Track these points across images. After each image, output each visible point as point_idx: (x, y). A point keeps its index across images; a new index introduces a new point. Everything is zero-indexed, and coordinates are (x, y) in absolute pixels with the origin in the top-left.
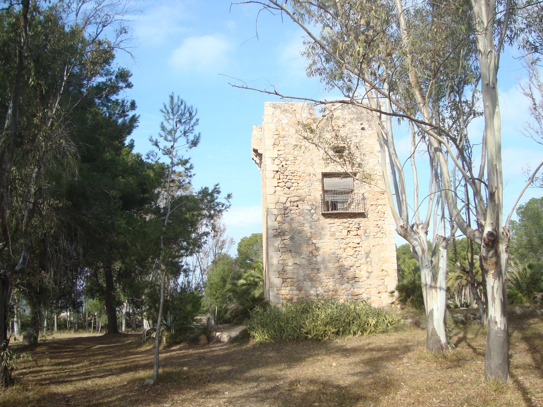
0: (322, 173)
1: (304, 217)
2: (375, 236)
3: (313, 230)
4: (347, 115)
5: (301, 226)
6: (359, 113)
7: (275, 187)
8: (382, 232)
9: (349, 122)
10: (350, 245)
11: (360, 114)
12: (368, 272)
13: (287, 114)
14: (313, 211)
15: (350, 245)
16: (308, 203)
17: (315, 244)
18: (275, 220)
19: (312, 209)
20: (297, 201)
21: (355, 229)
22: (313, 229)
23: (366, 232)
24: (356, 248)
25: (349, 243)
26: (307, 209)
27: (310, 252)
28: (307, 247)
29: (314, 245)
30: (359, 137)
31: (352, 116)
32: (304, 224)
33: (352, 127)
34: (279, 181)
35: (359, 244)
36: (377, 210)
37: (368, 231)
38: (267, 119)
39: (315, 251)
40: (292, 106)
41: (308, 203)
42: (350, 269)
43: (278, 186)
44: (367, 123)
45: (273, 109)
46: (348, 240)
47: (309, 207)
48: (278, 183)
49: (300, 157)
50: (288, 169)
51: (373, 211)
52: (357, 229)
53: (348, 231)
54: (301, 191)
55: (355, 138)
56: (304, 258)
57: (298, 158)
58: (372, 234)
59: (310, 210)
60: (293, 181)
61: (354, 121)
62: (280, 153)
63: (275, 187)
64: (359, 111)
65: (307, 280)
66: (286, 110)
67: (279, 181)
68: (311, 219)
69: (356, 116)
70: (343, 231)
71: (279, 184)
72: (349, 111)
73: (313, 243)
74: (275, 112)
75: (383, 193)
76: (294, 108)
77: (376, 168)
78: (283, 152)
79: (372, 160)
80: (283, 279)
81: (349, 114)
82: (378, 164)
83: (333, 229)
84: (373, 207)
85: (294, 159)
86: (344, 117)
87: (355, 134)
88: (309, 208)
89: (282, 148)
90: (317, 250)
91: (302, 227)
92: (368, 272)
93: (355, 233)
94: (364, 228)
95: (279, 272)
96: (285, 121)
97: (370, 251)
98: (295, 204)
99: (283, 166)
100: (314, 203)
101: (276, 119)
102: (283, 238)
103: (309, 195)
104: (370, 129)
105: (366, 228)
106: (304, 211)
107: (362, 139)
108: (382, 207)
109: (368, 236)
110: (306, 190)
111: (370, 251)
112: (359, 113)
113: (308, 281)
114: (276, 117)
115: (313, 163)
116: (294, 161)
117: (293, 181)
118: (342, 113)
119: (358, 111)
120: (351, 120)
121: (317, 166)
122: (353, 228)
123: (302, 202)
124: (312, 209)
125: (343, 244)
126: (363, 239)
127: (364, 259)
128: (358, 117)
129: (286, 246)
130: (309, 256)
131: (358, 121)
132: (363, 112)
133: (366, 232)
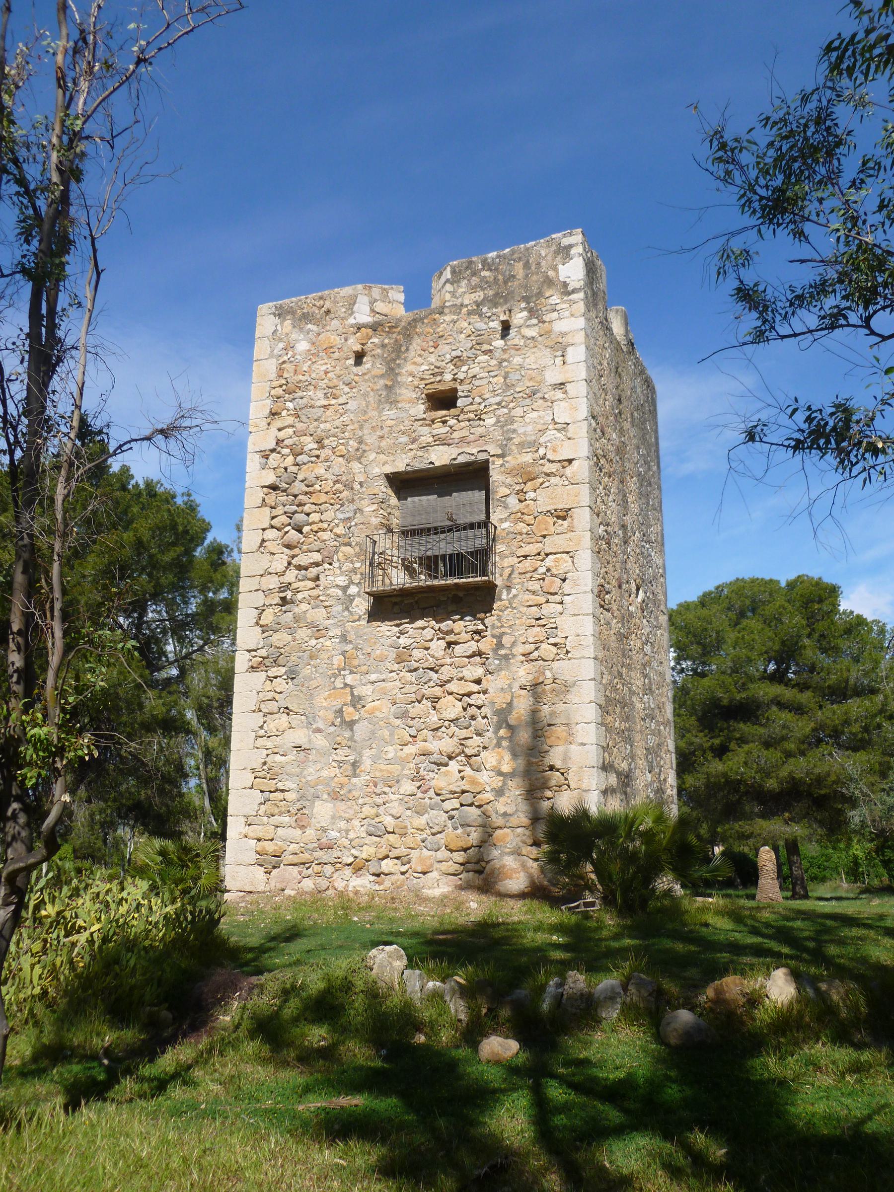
0: (387, 476)
1: (329, 609)
2: (531, 657)
3: (349, 647)
4: (467, 296)
5: (318, 635)
6: (501, 282)
7: (264, 530)
8: (552, 641)
9: (469, 313)
10: (451, 687)
11: (505, 282)
12: (500, 773)
13: (310, 326)
14: (353, 590)
15: (452, 687)
16: (340, 568)
17: (351, 687)
18: (257, 623)
19: (351, 582)
20: (317, 564)
21: (469, 636)
22: (351, 642)
23: (500, 645)
24: (469, 695)
25: (449, 681)
26: (337, 586)
27: (336, 712)
28: (330, 696)
29: (348, 689)
30: (498, 354)
31: (479, 295)
32: (326, 629)
33: (481, 325)
34: (275, 512)
35: (478, 682)
36: (542, 570)
37: (506, 640)
38: (261, 348)
39: (351, 709)
40: (322, 302)
41: (340, 568)
42: (446, 765)
43: (272, 527)
44: (523, 305)
45: (277, 320)
46: (446, 672)
47: (343, 578)
48: (273, 518)
49: (332, 439)
50: (300, 477)
51: (528, 575)
52: (477, 637)
53: (449, 644)
54: (325, 536)
55: (486, 357)
56: (318, 730)
57: (326, 442)
58: (520, 649)
59: (345, 589)
60: (307, 508)
61: (485, 309)
62: (281, 435)
63: (264, 530)
64: (503, 275)
65: (325, 796)
66: (306, 317)
67: (275, 512)
68: (346, 613)
69: (491, 293)
70: (433, 645)
71: (275, 522)
72: (475, 280)
73: (346, 685)
74: (279, 327)
75: (561, 514)
76: (328, 304)
77: (542, 440)
78: (290, 431)
79: (534, 415)
80: (262, 791)
81: (473, 289)
82: (551, 427)
83: (403, 641)
84: (527, 565)
85: (315, 446)
86: (459, 301)
87: (486, 347)
88: (342, 580)
89: (290, 420)
90: (354, 706)
91: (321, 640)
92: (500, 773)
93: (473, 646)
94: (495, 632)
95: (253, 770)
96: (303, 346)
97: (510, 705)
98: (313, 572)
99: (286, 469)
100: (358, 565)
101: (281, 345)
102: (270, 674)
103: (345, 545)
104: (535, 321)
105: (503, 630)
106: (332, 591)
107: (505, 356)
108: (556, 561)
109: (506, 657)
110: (339, 530)
111: (510, 705)
112: (501, 282)
113: (326, 801)
114: (281, 340)
115: (365, 451)
116: (317, 452)
117: (307, 508)
118: (453, 294)
119: (500, 277)
120: (478, 306)
121: (372, 456)
122: (463, 634)
123: (326, 566)
124: (351, 582)
125: (432, 684)
126: (491, 668)
127: (490, 734)
128: (496, 295)
129: (277, 696)
130: (333, 724)
131: (496, 305)
132: (514, 276)
133: (500, 645)
